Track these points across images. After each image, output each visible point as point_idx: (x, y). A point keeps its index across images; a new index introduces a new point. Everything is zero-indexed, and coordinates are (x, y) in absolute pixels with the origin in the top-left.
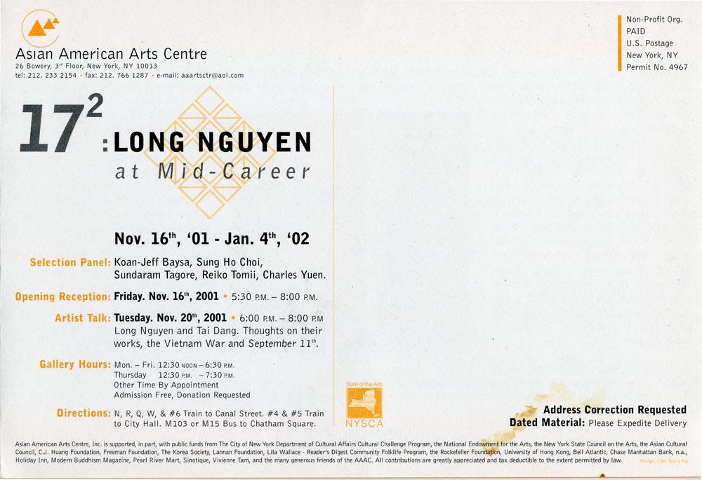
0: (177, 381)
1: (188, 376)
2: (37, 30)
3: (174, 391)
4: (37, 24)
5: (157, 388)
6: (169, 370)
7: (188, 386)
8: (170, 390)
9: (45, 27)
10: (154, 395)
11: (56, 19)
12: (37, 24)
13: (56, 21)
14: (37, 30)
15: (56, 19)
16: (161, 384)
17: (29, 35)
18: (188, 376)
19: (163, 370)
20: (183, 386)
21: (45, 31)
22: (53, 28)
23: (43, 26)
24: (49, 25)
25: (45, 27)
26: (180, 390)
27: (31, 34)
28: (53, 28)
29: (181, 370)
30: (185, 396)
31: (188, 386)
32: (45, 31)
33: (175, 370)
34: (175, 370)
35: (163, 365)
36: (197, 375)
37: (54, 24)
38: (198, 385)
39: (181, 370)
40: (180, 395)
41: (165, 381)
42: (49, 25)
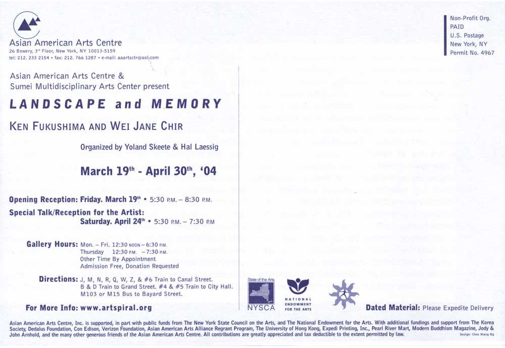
0: (126, 256)
1: (134, 252)
3: (123, 264)
5: (111, 261)
6: (120, 249)
7: (133, 259)
8: (120, 263)
10: (109, 266)
16: (114, 259)
18: (134, 252)
19: (115, 248)
20: (130, 260)
26: (128, 262)
29: (129, 248)
30: (132, 267)
31: (133, 259)
33: (124, 248)
34: (124, 248)
35: (115, 245)
36: (140, 252)
38: (141, 259)
39: (129, 248)
40: (128, 266)
41: (117, 256)
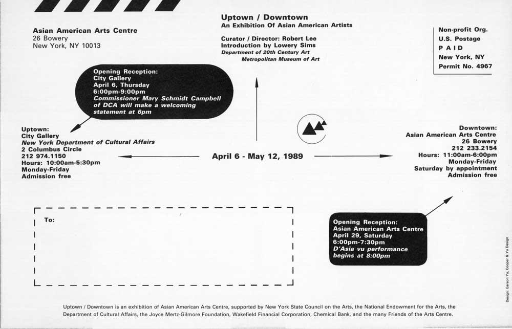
2: (309, 130)
4: (309, 126)
9: (316, 129)
11: (324, 121)
12: (309, 126)
13: (324, 123)
14: (309, 130)
15: (324, 121)
17: (305, 133)
21: (316, 131)
22: (323, 129)
23: (314, 127)
24: (320, 127)
25: (316, 129)
27: (305, 133)
28: (323, 129)
32: (316, 131)
37: (323, 126)
42: (320, 127)
